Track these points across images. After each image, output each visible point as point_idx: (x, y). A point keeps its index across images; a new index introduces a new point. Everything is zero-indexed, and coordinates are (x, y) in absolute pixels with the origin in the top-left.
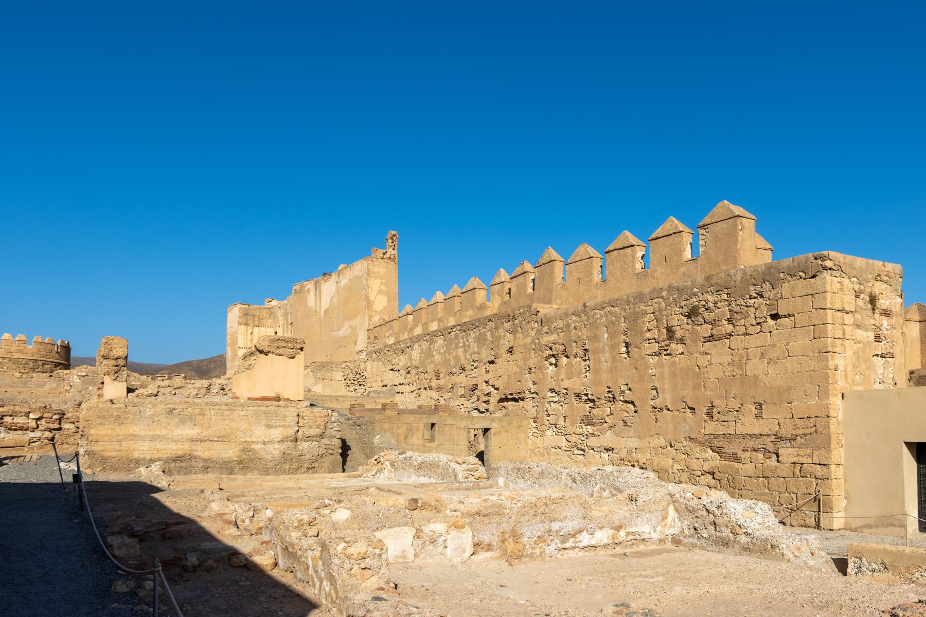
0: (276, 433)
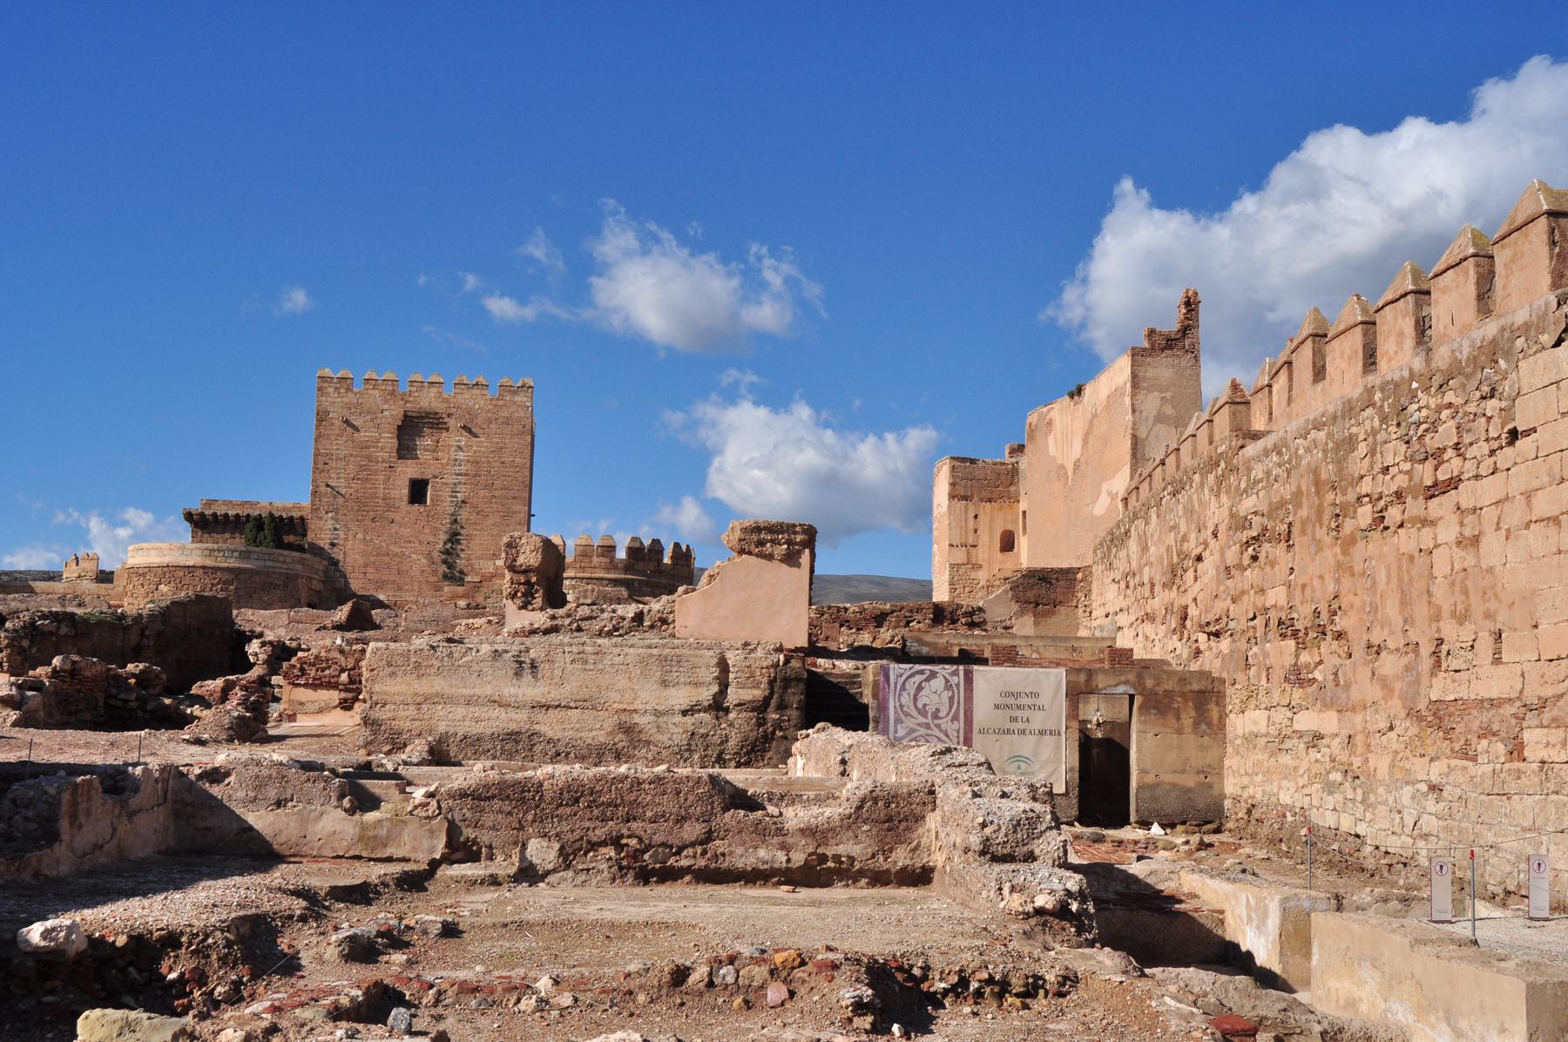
0: (680, 697)
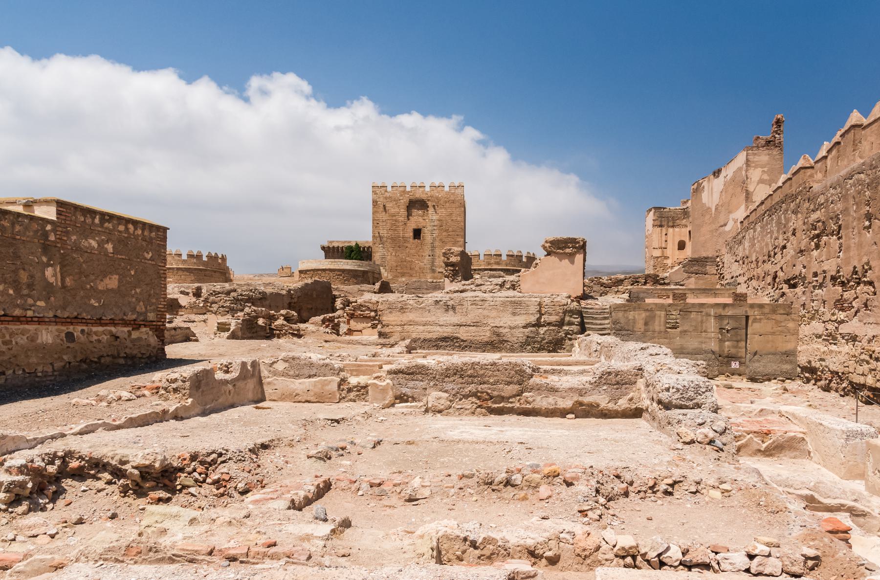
0: (521, 320)
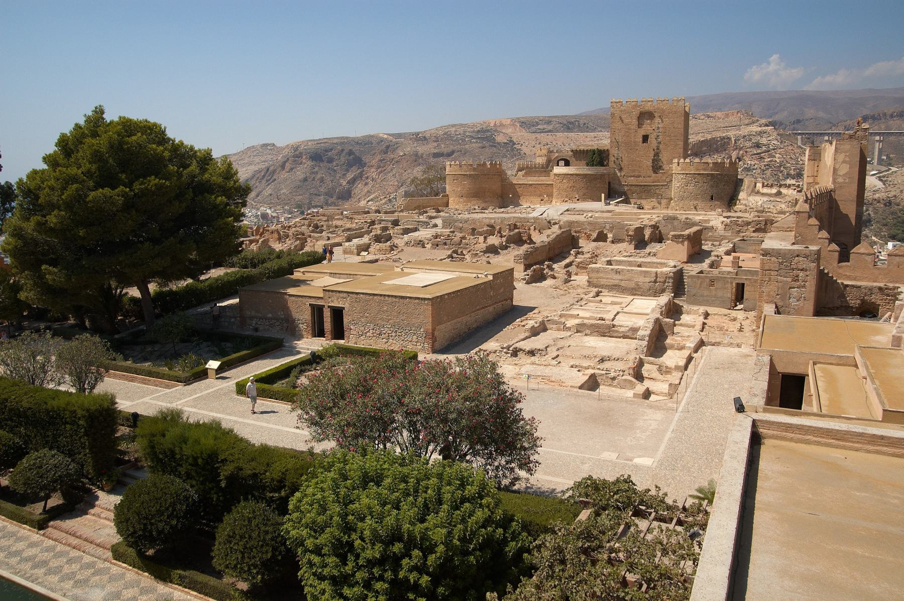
0: (648, 280)
